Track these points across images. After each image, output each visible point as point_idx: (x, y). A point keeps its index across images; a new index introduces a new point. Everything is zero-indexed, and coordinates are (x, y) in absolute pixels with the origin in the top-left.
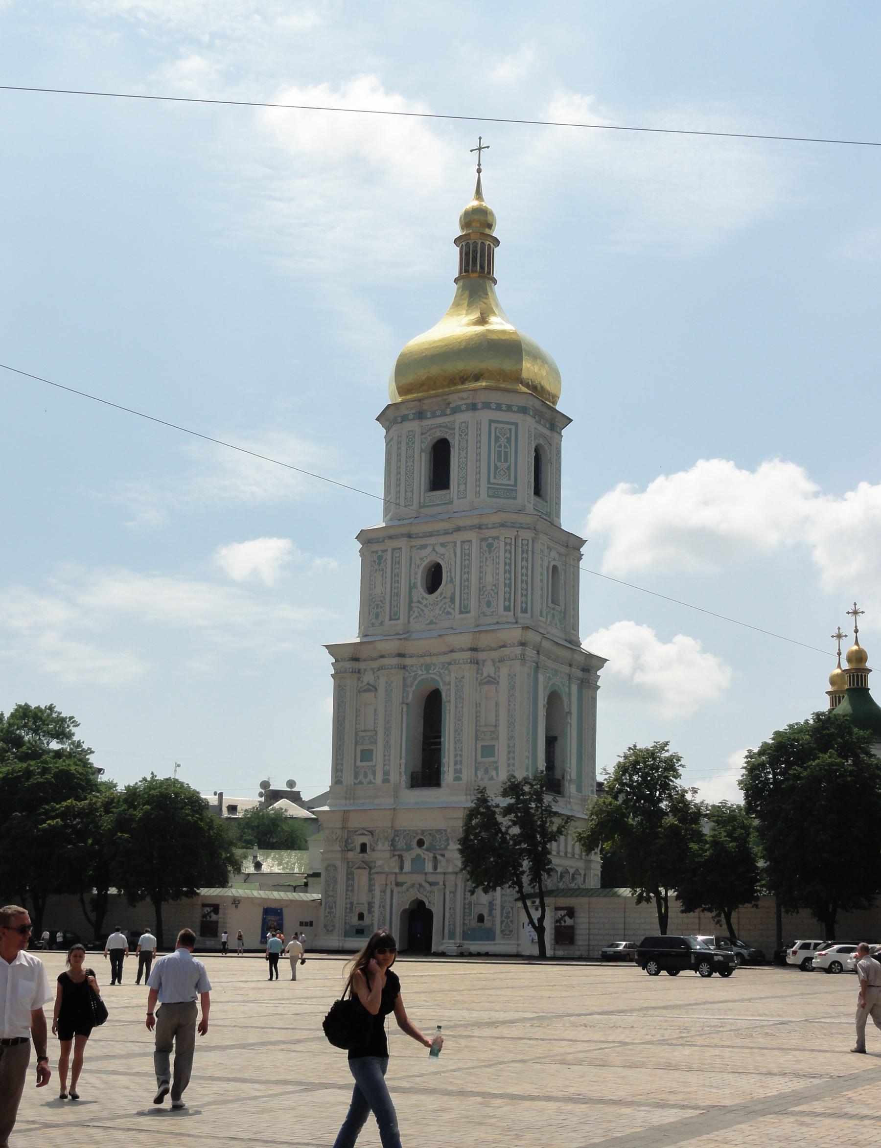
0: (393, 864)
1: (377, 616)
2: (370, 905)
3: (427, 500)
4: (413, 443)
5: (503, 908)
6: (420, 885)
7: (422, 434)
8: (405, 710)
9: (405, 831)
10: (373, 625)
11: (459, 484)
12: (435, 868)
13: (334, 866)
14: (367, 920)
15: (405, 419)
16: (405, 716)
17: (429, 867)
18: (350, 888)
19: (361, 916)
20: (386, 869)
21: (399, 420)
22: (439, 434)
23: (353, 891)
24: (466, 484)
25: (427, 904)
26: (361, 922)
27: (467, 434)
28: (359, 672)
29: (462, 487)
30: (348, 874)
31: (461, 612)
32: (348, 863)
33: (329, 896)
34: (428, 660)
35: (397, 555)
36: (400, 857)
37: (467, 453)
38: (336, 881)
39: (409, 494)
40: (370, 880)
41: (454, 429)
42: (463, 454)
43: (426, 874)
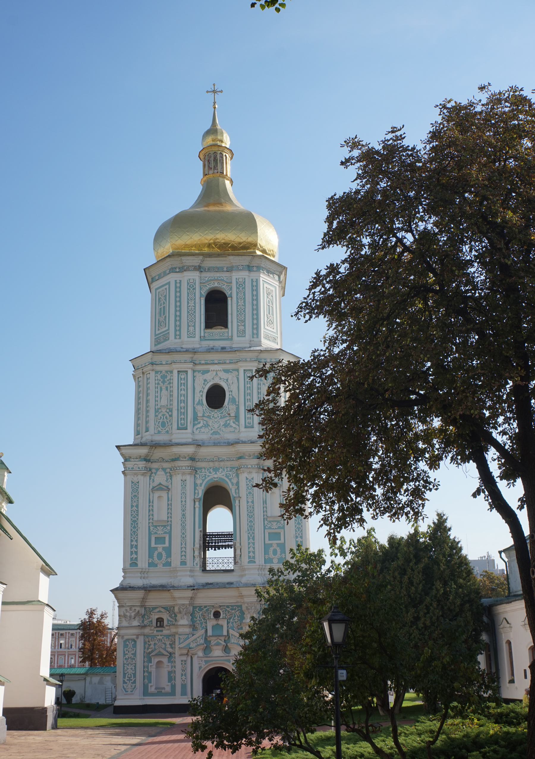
1: (163, 425)
3: (206, 335)
4: (195, 289)
7: (201, 283)
8: (197, 503)
10: (159, 432)
11: (238, 326)
15: (182, 269)
16: (197, 510)
21: (178, 270)
22: (215, 285)
24: (244, 326)
27: (244, 288)
28: (150, 470)
29: (242, 328)
31: (246, 427)
34: (217, 464)
35: (183, 377)
37: (244, 302)
39: (191, 329)
41: (231, 283)
42: (241, 303)
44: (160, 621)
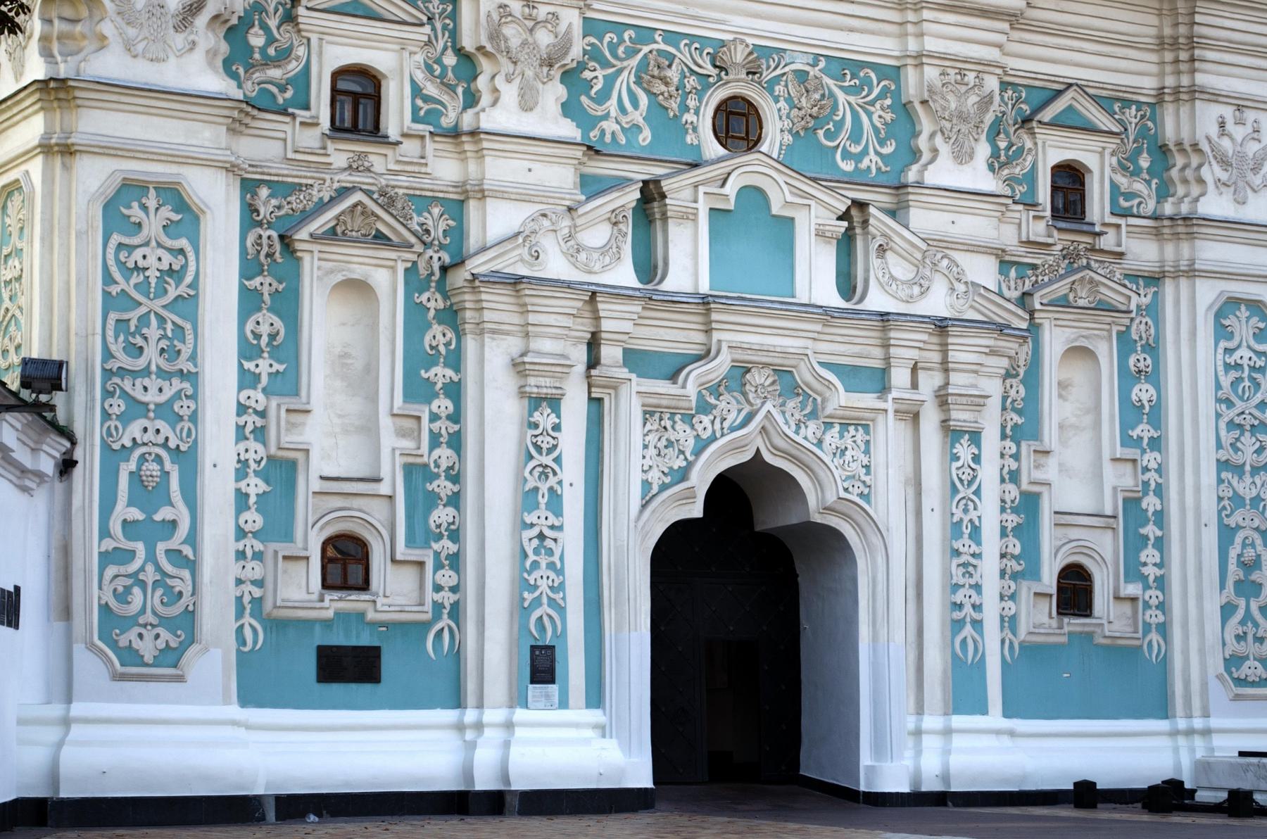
0: (597, 235)
2: (434, 488)
5: (1226, 534)
6: (786, 382)
9: (645, 34)
12: (847, 284)
13: (173, 195)
14: (393, 591)
17: (816, 277)
18: (264, 366)
19: (346, 561)
20: (556, 265)
23: (288, 383)
25: (819, 499)
26: (352, 602)
30: (250, 267)
32: (249, 187)
33: (137, 408)
36: (651, 194)
38: (188, 304)
40: (416, 319)
43: (827, 314)
44: (358, 101)
